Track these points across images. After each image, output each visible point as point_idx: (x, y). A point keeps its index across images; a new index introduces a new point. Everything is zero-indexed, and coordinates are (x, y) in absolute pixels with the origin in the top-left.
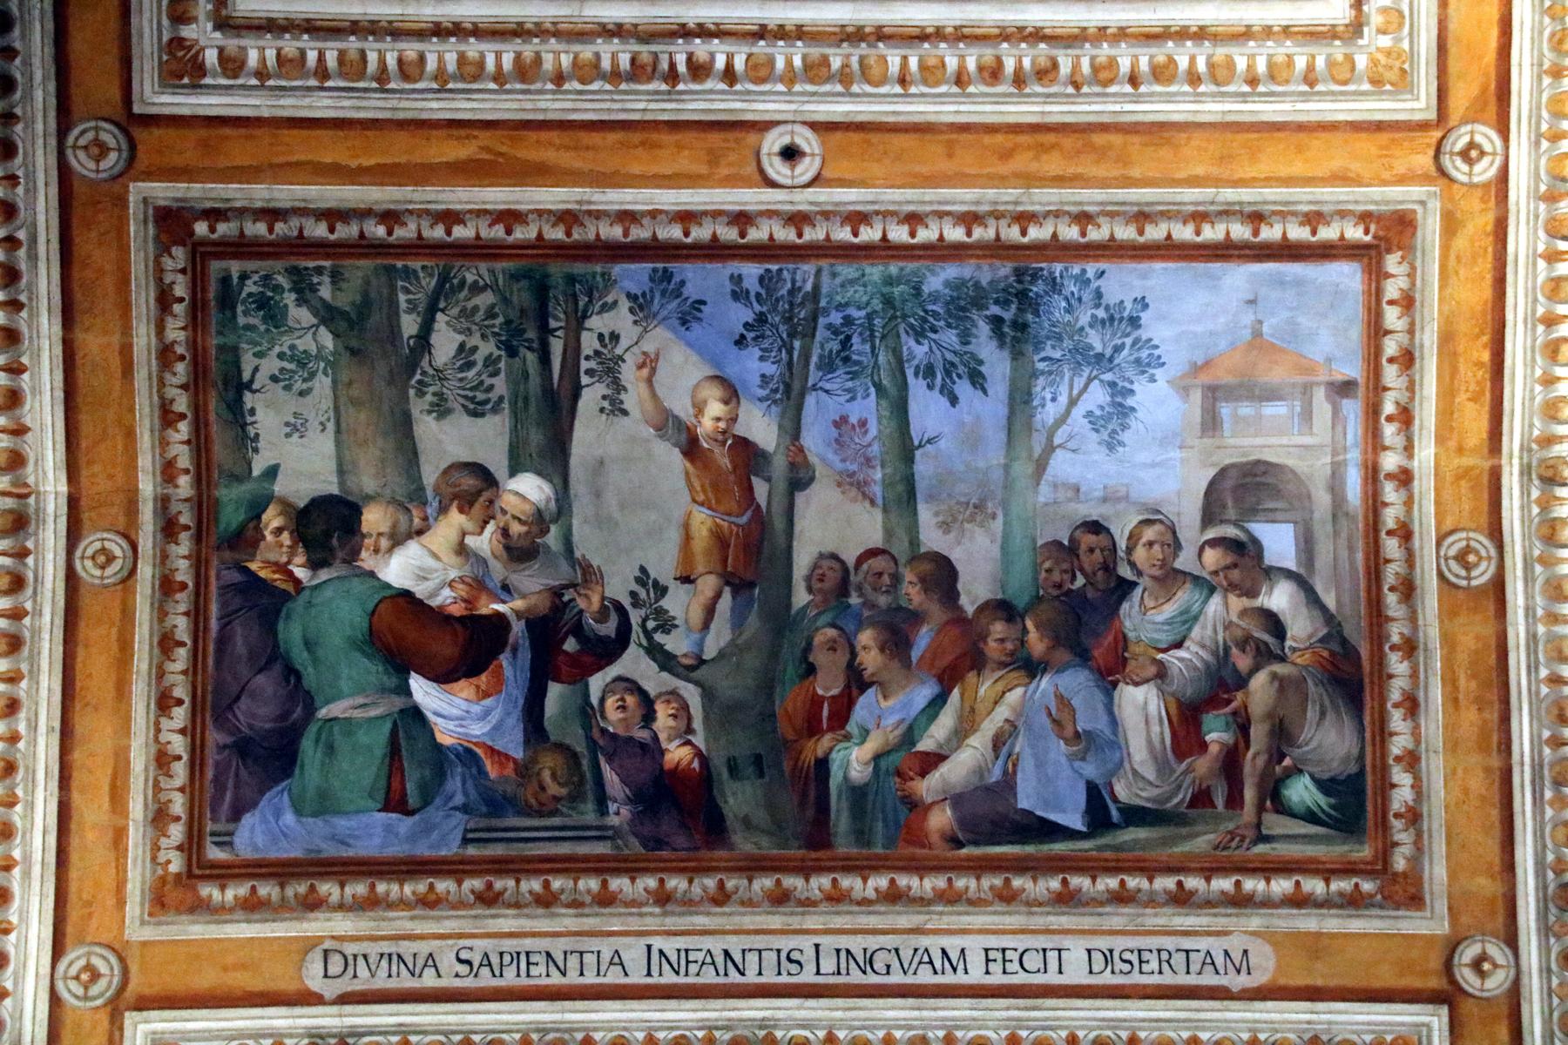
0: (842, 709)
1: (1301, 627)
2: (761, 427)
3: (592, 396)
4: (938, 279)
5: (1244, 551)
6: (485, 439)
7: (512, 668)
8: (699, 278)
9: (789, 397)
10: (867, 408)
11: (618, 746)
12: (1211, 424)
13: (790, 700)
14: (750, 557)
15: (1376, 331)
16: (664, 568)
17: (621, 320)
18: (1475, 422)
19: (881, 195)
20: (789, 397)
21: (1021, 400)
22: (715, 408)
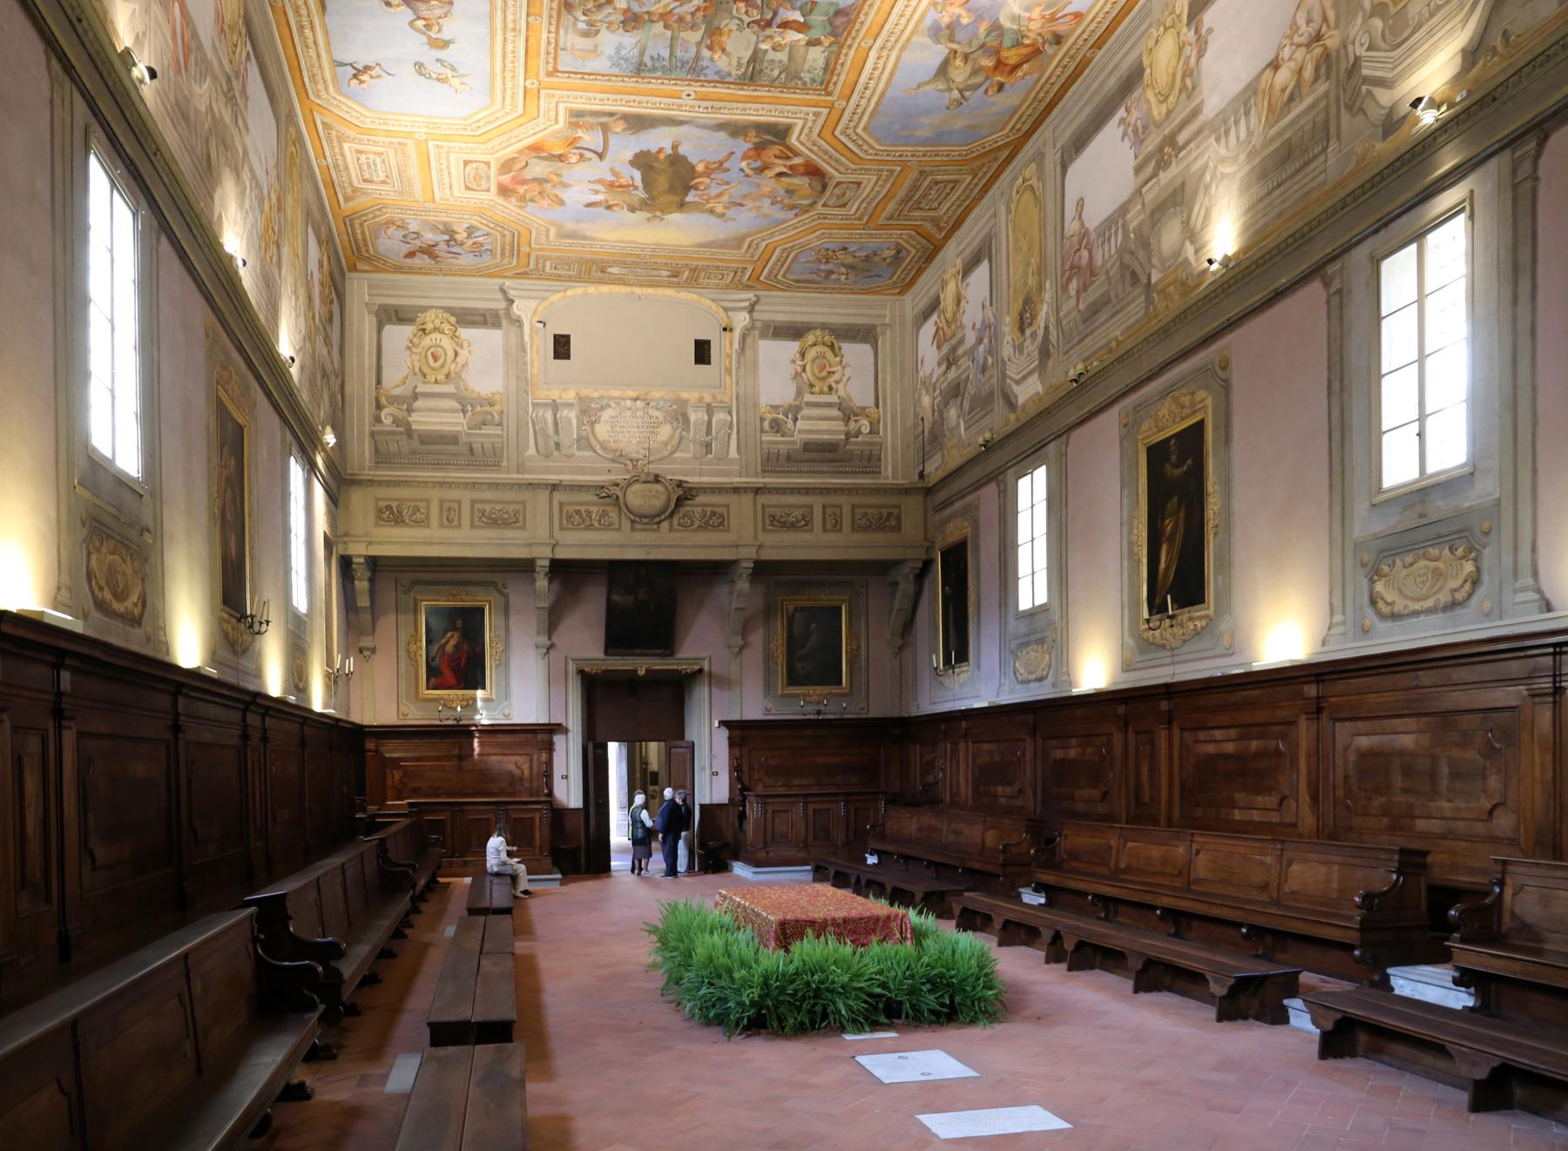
0: (698, 9)
1: (579, 14)
2: (706, 53)
3: (745, 61)
4: (659, 74)
5: (590, 24)
6: (771, 55)
7: (778, 20)
8: (716, 78)
9: (698, 57)
10: (679, 54)
11: (756, 7)
12: (596, 46)
13: (709, 12)
14: (713, 32)
15: (555, 58)
16: (736, 33)
17: (734, 73)
18: (531, 40)
19: (668, 87)
20: (698, 57)
21: (642, 53)
22: (716, 57)
